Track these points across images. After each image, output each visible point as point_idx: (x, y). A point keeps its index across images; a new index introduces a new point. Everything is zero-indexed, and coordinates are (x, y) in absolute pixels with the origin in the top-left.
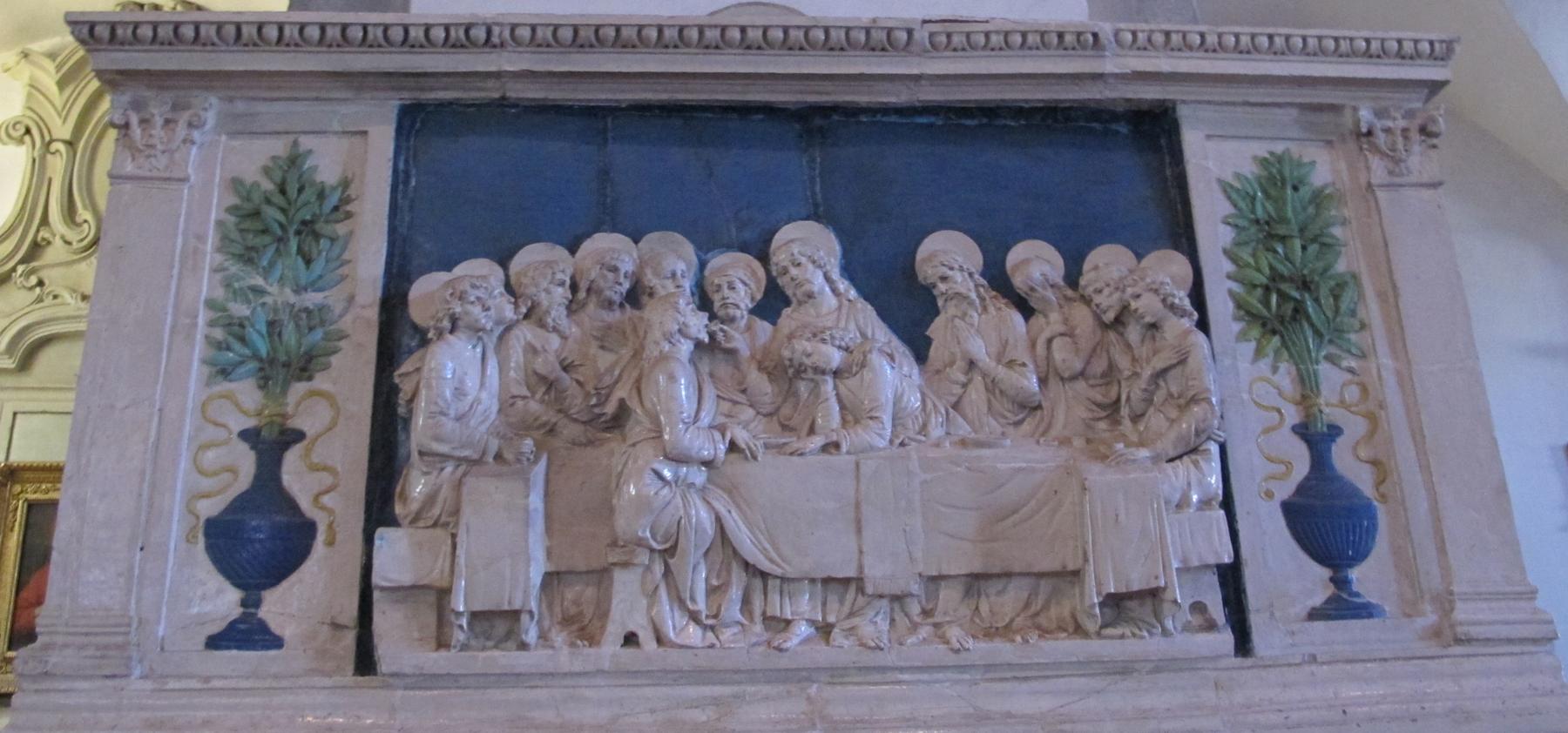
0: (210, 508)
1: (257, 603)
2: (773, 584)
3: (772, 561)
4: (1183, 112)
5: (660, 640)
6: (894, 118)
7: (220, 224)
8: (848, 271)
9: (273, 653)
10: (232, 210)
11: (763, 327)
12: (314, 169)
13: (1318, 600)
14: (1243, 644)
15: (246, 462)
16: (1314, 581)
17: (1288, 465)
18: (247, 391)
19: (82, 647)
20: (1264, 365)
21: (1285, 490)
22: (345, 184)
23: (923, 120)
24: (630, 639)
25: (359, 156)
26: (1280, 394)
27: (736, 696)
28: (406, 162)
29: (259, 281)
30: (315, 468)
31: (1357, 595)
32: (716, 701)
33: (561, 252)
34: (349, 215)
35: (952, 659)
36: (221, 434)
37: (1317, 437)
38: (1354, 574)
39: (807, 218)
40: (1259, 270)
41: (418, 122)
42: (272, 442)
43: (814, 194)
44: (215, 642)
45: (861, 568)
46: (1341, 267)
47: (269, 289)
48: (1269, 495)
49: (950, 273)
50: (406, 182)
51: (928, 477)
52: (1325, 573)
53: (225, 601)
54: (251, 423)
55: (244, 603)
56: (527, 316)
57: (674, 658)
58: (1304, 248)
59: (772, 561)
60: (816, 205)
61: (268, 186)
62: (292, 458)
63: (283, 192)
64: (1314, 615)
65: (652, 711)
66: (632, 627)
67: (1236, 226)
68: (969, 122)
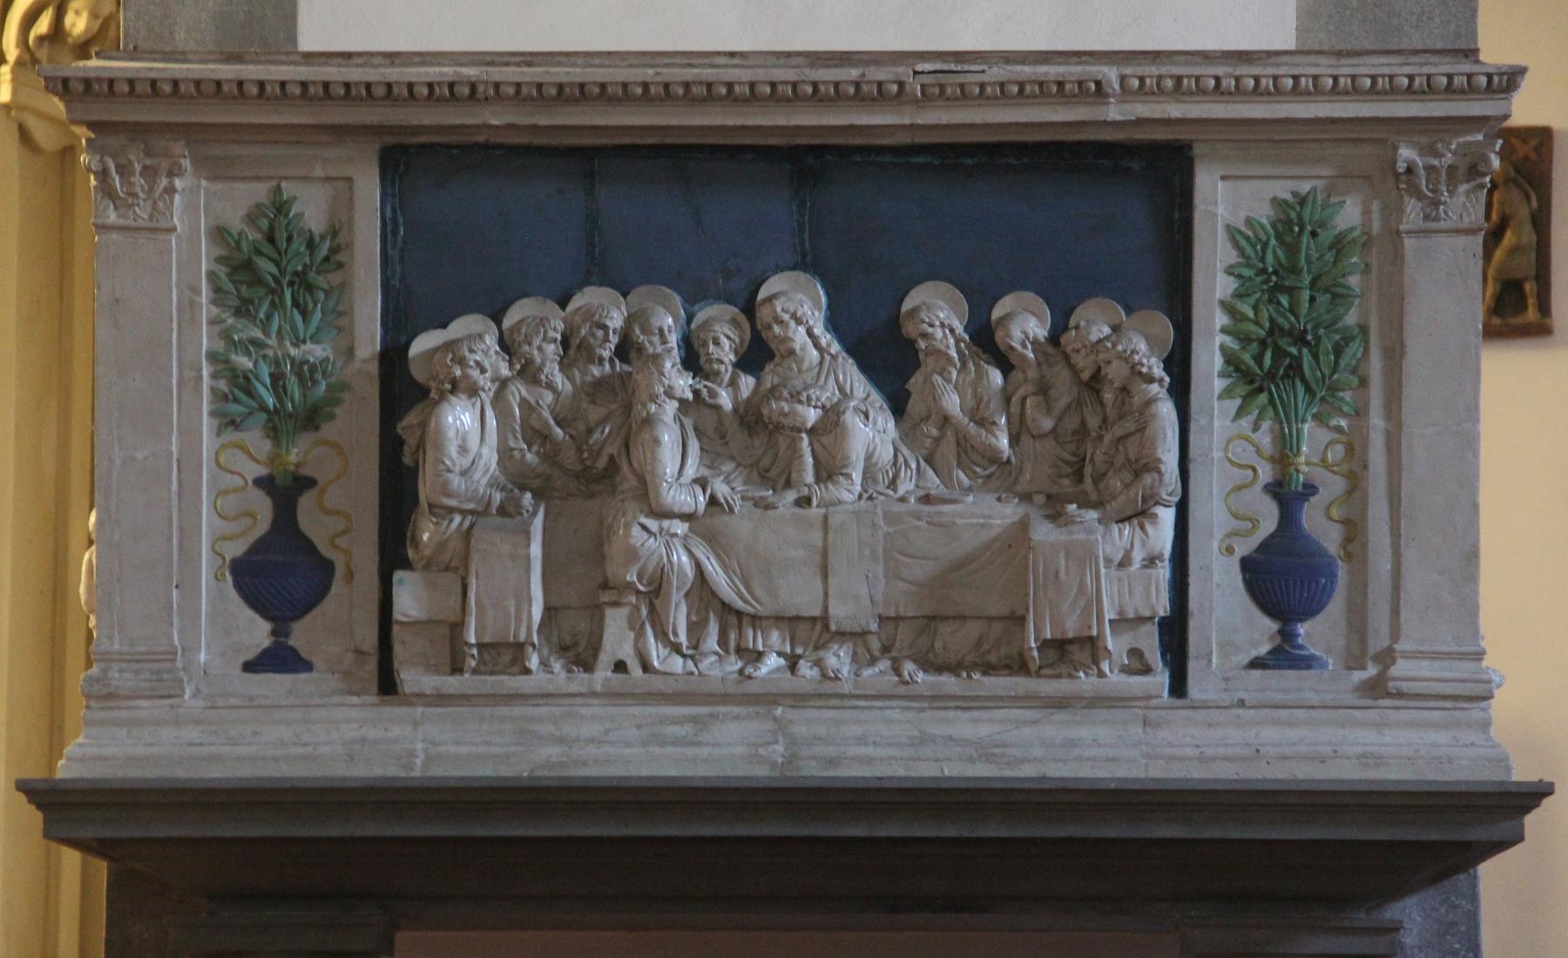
0: (236, 549)
1: (287, 635)
2: (745, 621)
3: (746, 601)
4: (1198, 149)
5: (646, 667)
6: (888, 158)
7: (211, 275)
8: (833, 324)
9: (303, 676)
10: (219, 260)
11: (747, 383)
12: (300, 216)
13: (1263, 650)
14: (1179, 687)
15: (263, 507)
16: (1261, 631)
17: (1255, 522)
18: (255, 438)
19: (137, 672)
20: (1246, 423)
21: (1244, 548)
22: (333, 232)
23: (921, 160)
24: (620, 667)
25: (346, 202)
26: (1258, 452)
27: (712, 715)
28: (394, 209)
29: (257, 333)
30: (328, 512)
31: (1301, 647)
32: (695, 720)
33: (551, 307)
34: (340, 265)
35: (902, 690)
36: (238, 481)
37: (1288, 496)
38: (1302, 629)
39: (794, 268)
40: (1257, 323)
41: (401, 160)
42: (285, 490)
43: (802, 243)
44: (249, 667)
45: (826, 608)
46: (1351, 319)
47: (269, 342)
48: (1230, 550)
49: (930, 330)
50: (395, 233)
51: (891, 530)
52: (1272, 626)
53: (258, 633)
54: (262, 471)
55: (274, 633)
56: (521, 373)
57: (657, 683)
58: (1312, 299)
59: (746, 601)
60: (804, 255)
61: (253, 235)
62: (306, 503)
63: (271, 239)
64: (1256, 664)
65: (638, 727)
66: (621, 656)
67: (1239, 276)
68: (969, 161)
